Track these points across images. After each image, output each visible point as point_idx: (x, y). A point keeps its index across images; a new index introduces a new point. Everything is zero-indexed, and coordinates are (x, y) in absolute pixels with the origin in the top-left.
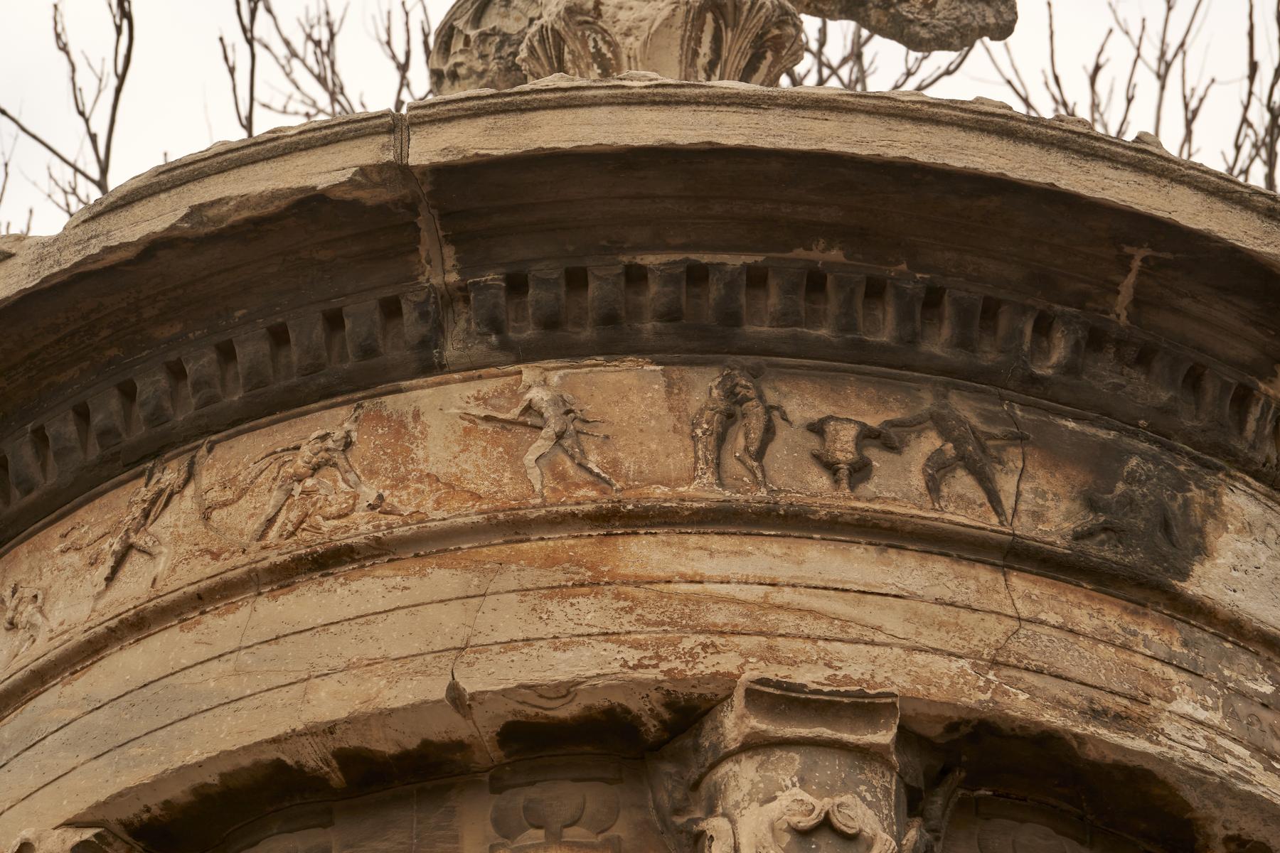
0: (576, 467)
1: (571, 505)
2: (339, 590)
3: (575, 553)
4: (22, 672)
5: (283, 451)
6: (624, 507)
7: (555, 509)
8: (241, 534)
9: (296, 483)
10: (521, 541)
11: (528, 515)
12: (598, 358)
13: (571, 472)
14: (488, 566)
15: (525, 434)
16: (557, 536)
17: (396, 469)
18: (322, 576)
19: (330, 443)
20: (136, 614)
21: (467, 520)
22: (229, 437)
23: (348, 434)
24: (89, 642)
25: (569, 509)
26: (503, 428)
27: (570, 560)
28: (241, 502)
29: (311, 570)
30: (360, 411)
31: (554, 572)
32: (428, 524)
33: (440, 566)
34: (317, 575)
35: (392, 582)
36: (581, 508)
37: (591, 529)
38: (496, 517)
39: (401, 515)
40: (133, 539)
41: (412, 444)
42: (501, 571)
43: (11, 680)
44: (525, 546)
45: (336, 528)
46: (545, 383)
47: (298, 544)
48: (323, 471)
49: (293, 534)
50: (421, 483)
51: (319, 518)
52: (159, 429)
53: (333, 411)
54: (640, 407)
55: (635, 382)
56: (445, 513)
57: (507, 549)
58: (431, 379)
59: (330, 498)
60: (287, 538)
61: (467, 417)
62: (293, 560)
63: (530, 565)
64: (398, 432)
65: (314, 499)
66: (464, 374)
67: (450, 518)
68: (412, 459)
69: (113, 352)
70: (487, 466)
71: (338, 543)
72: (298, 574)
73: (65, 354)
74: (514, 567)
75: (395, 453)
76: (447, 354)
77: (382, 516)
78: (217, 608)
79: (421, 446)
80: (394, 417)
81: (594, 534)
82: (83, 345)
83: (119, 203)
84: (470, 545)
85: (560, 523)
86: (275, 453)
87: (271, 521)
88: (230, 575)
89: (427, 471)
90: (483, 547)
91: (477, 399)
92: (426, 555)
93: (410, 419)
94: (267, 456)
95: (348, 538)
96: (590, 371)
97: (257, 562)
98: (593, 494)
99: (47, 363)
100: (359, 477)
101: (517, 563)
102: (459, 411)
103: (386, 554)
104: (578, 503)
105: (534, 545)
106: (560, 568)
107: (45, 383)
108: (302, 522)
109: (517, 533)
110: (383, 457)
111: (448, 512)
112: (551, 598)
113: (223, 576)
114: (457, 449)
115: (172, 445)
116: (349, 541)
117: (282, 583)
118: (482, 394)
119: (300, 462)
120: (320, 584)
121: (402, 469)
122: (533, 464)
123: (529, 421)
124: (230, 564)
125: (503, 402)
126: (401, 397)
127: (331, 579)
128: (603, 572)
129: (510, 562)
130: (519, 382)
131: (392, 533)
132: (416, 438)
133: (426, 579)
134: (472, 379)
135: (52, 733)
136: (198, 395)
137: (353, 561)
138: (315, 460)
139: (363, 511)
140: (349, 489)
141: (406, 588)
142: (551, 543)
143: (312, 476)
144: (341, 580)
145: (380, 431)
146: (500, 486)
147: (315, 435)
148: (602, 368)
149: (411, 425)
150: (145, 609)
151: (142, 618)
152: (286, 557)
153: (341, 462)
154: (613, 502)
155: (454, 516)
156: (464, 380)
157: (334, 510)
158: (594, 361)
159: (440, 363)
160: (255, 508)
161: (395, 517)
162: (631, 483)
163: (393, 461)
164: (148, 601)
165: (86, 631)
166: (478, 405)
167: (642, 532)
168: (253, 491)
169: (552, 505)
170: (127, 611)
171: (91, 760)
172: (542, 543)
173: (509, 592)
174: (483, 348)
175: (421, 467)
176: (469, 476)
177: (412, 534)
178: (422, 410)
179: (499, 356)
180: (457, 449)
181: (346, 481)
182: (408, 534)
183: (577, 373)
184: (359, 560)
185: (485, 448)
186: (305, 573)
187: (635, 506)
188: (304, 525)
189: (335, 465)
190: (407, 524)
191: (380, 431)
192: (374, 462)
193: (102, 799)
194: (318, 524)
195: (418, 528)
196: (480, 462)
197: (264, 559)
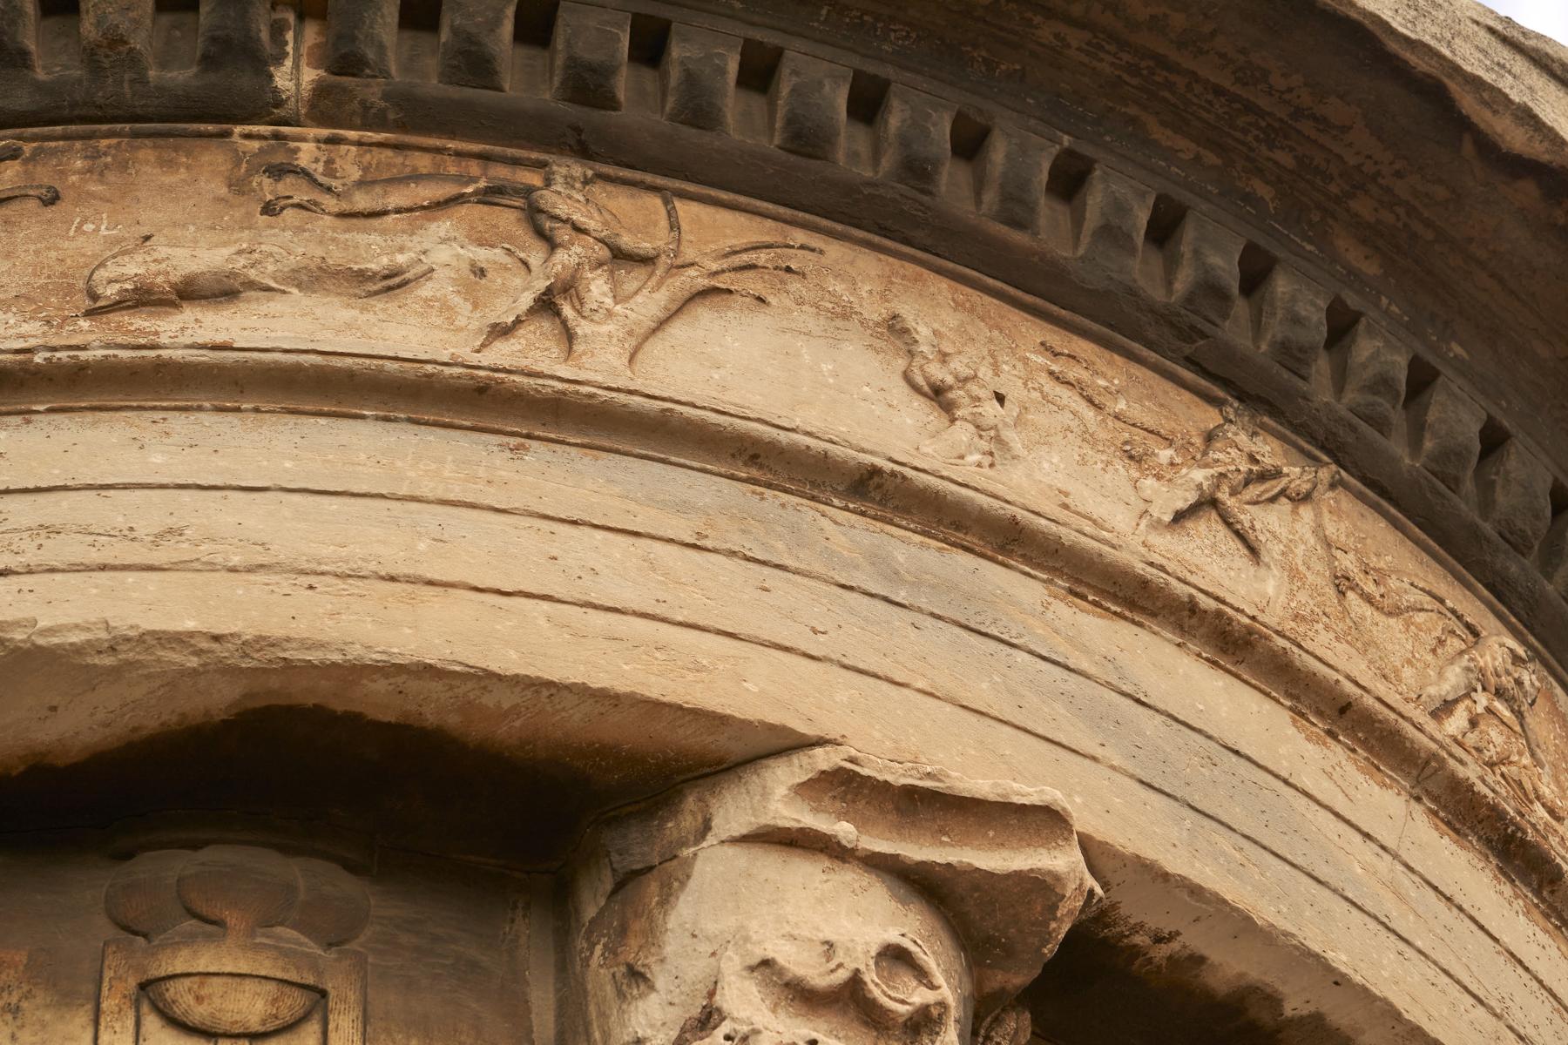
4: (996, 504)
5: (1453, 612)
20: (1250, 631)
22: (1360, 497)
24: (1144, 584)
40: (1223, 495)
43: (964, 491)
52: (1286, 375)
69: (1264, 191)
73: (1205, 115)
78: (1353, 751)
82: (1238, 135)
83: (1555, 66)
86: (1442, 601)
94: (1430, 593)
99: (1167, 94)
107: (1133, 110)
115: (1275, 411)
135: (1031, 652)
136: (1371, 398)
150: (1267, 638)
151: (1248, 643)
164: (1278, 633)
165: (1151, 564)
170: (1237, 610)
171: (1132, 776)
193: (1170, 869)
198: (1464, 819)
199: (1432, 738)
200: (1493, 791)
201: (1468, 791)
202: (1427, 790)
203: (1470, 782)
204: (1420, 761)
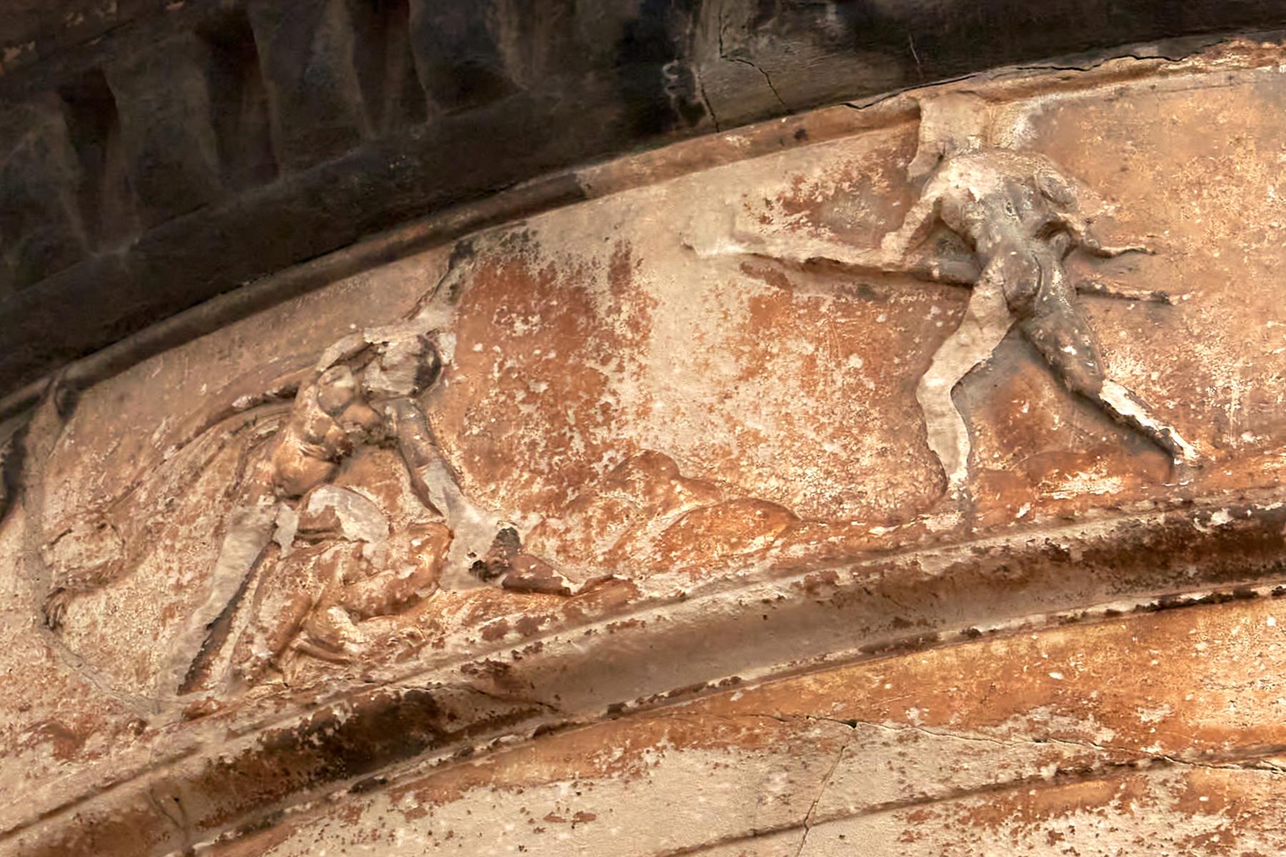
0: (1068, 403)
1: (1046, 526)
2: (401, 833)
3: (1068, 672)
5: (254, 404)
6: (1205, 520)
7: (1001, 541)
8: (142, 673)
9: (285, 506)
10: (913, 646)
11: (924, 567)
12: (1144, 50)
13: (1056, 420)
14: (815, 733)
15: (926, 308)
16: (1016, 623)
17: (560, 443)
18: (356, 790)
19: (376, 379)
21: (748, 596)
23: (428, 344)
25: (1040, 538)
26: (864, 292)
27: (1052, 698)
28: (144, 569)
29: (326, 775)
30: (465, 266)
31: (1006, 737)
32: (639, 616)
33: (679, 742)
34: (341, 791)
35: (541, 802)
36: (1074, 532)
37: (1117, 593)
38: (830, 581)
39: (564, 593)
41: (605, 362)
42: (852, 746)
44: (925, 660)
45: (383, 643)
46: (989, 144)
47: (279, 701)
48: (364, 463)
49: (271, 666)
50: (625, 485)
51: (338, 615)
53: (392, 273)
54: (1262, 196)
55: (1251, 116)
56: (686, 578)
57: (872, 675)
58: (661, 155)
59: (367, 550)
60: (252, 683)
61: (761, 266)
62: (270, 750)
63: (936, 720)
64: (568, 324)
65: (327, 556)
66: (757, 130)
67: (701, 592)
68: (605, 409)
70: (812, 418)
71: (389, 690)
72: (291, 789)
74: (889, 730)
75: (558, 396)
76: (700, 73)
77: (511, 597)
79: (631, 367)
80: (561, 278)
81: (1122, 606)
84: (766, 671)
85: (1023, 582)
87: (218, 628)
88: (102, 805)
89: (645, 446)
90: (802, 672)
91: (791, 206)
92: (647, 709)
93: (603, 284)
95: (417, 672)
96: (1121, 93)
97: (172, 761)
98: (1109, 486)
100: (455, 477)
101: (899, 718)
102: (739, 249)
103: (531, 713)
104: (1067, 519)
105: (950, 657)
106: (1022, 724)
108: (297, 629)
109: (899, 623)
110: (525, 409)
111: (694, 572)
112: (995, 822)
113: (85, 807)
114: (728, 369)
116: (420, 683)
117: (246, 819)
118: (805, 188)
119: (293, 442)
120: (353, 815)
121: (578, 444)
122: (946, 403)
123: (936, 267)
124: (101, 768)
125: (864, 212)
126: (582, 212)
127: (381, 799)
128: (1146, 727)
129: (878, 716)
130: (910, 144)
131: (538, 648)
132: (617, 342)
133: (640, 786)
134: (780, 143)
137: (442, 739)
138: (333, 429)
139: (463, 584)
140: (427, 519)
141: (583, 817)
142: (999, 647)
143: (329, 480)
144: (409, 801)
145: (519, 327)
146: (852, 478)
147: (331, 355)
148: (1155, 80)
149: (604, 304)
152: (250, 742)
153: (415, 435)
154: (1170, 507)
155: (710, 588)
156: (756, 151)
157: (372, 588)
158: (1131, 62)
159: (682, 101)
160: (179, 587)
161: (545, 600)
162: (1230, 440)
163: (552, 419)
166: (795, 226)
167: (1264, 590)
168: (174, 535)
169: (989, 531)
172: (972, 649)
173: (872, 810)
174: (800, 51)
175: (629, 433)
176: (763, 452)
177: (594, 651)
178: (638, 252)
179: (848, 69)
180: (728, 369)
181: (421, 492)
182: (581, 649)
183: (1084, 103)
184: (456, 736)
185: (812, 360)
186: (310, 785)
187: (1236, 513)
188: (301, 640)
189: (390, 443)
190: (575, 618)
191: (519, 327)
192: (500, 426)
194: (334, 635)
195: (611, 629)
196: (795, 407)
197: (191, 751)
198: (270, 792)
199: (134, 775)
200: (255, 728)
201: (226, 774)
202: (202, 823)
203: (215, 763)
204: (152, 814)
